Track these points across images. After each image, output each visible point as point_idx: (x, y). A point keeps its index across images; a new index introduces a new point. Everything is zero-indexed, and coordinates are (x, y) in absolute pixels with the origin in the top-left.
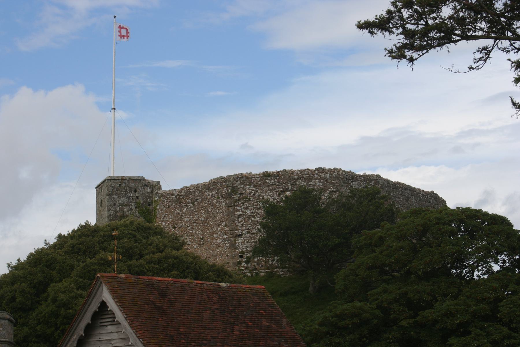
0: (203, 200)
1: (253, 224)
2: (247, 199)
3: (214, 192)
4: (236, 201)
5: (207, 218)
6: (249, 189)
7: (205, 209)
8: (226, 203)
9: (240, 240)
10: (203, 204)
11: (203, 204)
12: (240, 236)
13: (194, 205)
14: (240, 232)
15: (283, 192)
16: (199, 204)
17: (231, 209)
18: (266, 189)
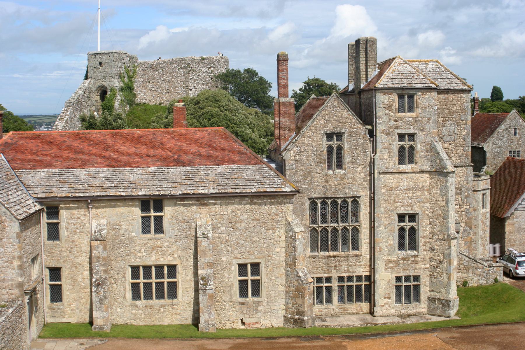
0: (169, 69)
1: (197, 84)
2: (194, 71)
3: (176, 65)
4: (189, 71)
5: (172, 79)
6: (195, 65)
7: (171, 75)
8: (184, 72)
9: (191, 92)
10: (169, 71)
11: (169, 71)
12: (191, 90)
13: (162, 70)
14: (191, 88)
15: (210, 68)
16: (166, 71)
17: (186, 75)
18: (202, 65)
